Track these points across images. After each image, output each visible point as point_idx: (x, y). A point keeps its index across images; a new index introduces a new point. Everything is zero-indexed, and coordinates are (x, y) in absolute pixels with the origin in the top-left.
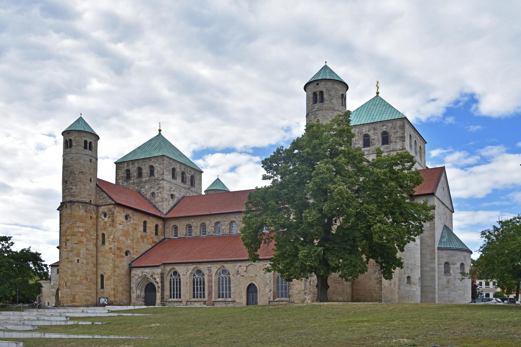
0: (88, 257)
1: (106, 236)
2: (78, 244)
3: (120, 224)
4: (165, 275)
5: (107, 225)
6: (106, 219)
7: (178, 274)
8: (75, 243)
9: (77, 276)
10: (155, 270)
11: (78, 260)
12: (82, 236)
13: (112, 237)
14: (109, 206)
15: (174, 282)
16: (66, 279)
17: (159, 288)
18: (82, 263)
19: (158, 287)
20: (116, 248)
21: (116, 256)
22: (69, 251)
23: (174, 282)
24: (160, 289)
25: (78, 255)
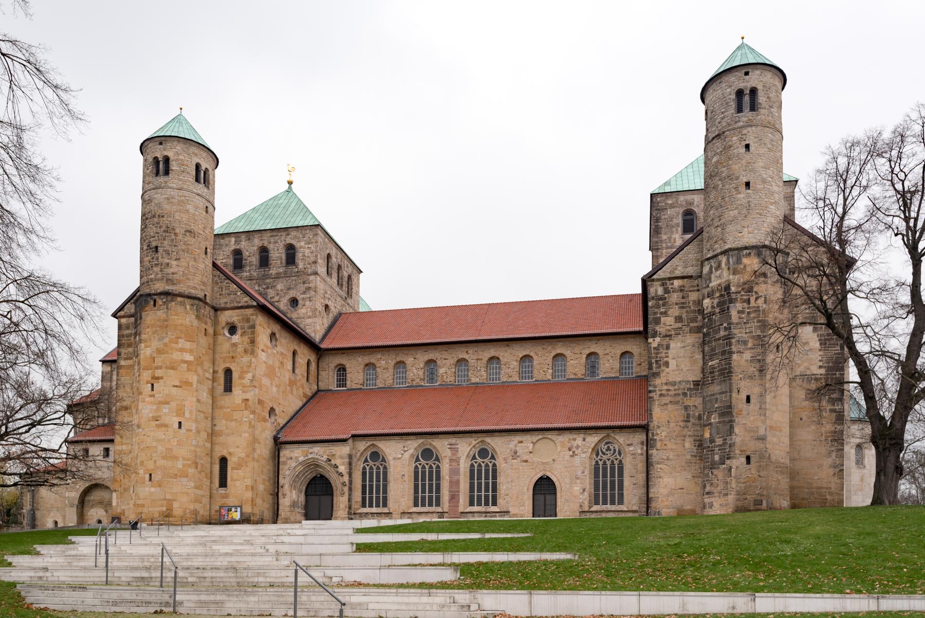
0: (199, 417)
1: (235, 375)
2: (180, 387)
3: (263, 351)
4: (355, 460)
5: (239, 350)
6: (236, 338)
7: (381, 457)
8: (174, 386)
9: (176, 458)
10: (336, 448)
11: (180, 423)
12: (189, 370)
13: (249, 376)
14: (243, 310)
15: (371, 474)
16: (150, 465)
17: (346, 485)
18: (188, 430)
19: (344, 484)
20: (257, 402)
21: (256, 416)
22: (161, 403)
23: (371, 474)
24: (346, 489)
25: (180, 411)
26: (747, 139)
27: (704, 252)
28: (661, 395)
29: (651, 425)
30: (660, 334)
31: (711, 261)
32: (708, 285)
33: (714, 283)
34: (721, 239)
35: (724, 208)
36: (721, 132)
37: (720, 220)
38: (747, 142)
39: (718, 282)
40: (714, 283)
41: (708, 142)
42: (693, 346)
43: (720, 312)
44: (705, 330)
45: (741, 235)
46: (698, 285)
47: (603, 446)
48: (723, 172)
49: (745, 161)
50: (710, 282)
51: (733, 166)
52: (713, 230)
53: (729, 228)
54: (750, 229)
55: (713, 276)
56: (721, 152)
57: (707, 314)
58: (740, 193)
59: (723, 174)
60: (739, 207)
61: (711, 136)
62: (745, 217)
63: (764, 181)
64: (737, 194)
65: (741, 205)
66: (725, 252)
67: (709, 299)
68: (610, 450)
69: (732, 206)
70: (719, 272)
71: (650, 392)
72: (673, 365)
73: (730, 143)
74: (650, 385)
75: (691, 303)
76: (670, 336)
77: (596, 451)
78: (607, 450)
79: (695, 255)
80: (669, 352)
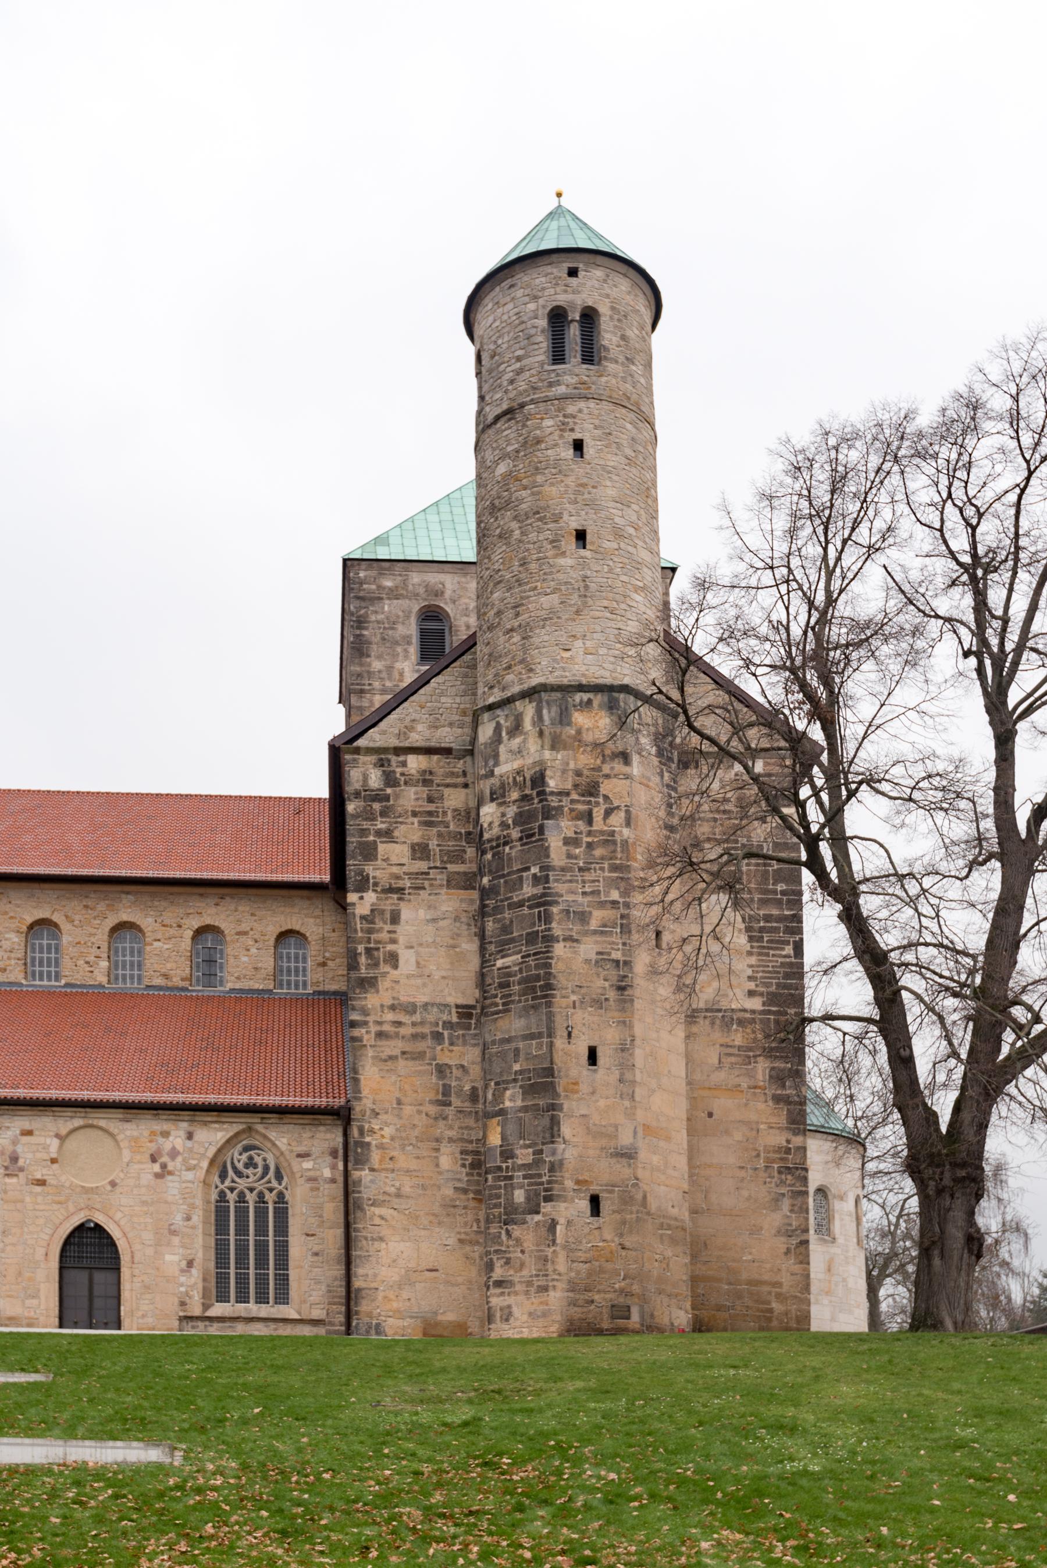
26: (577, 428)
27: (480, 692)
28: (380, 1035)
29: (357, 1107)
30: (376, 884)
31: (498, 712)
32: (492, 772)
33: (506, 767)
34: (521, 662)
35: (527, 587)
36: (515, 405)
37: (517, 615)
38: (578, 436)
39: (516, 765)
40: (506, 767)
41: (484, 426)
42: (457, 919)
43: (521, 839)
44: (485, 880)
45: (567, 655)
46: (464, 774)
47: (236, 1155)
48: (521, 501)
49: (572, 478)
50: (497, 764)
51: (547, 488)
52: (502, 639)
53: (539, 636)
54: (588, 644)
55: (502, 749)
56: (517, 452)
57: (489, 841)
58: (563, 554)
59: (523, 506)
60: (563, 588)
61: (492, 412)
62: (578, 612)
63: (618, 534)
64: (556, 556)
65: (566, 583)
66: (530, 694)
67: (494, 805)
68: (255, 1166)
69: (545, 585)
70: (518, 740)
71: (353, 1024)
72: (407, 961)
73: (538, 432)
74: (354, 1009)
75: (450, 814)
76: (400, 890)
77: (220, 1167)
78: (247, 1166)
79: (458, 700)
80: (399, 929)
